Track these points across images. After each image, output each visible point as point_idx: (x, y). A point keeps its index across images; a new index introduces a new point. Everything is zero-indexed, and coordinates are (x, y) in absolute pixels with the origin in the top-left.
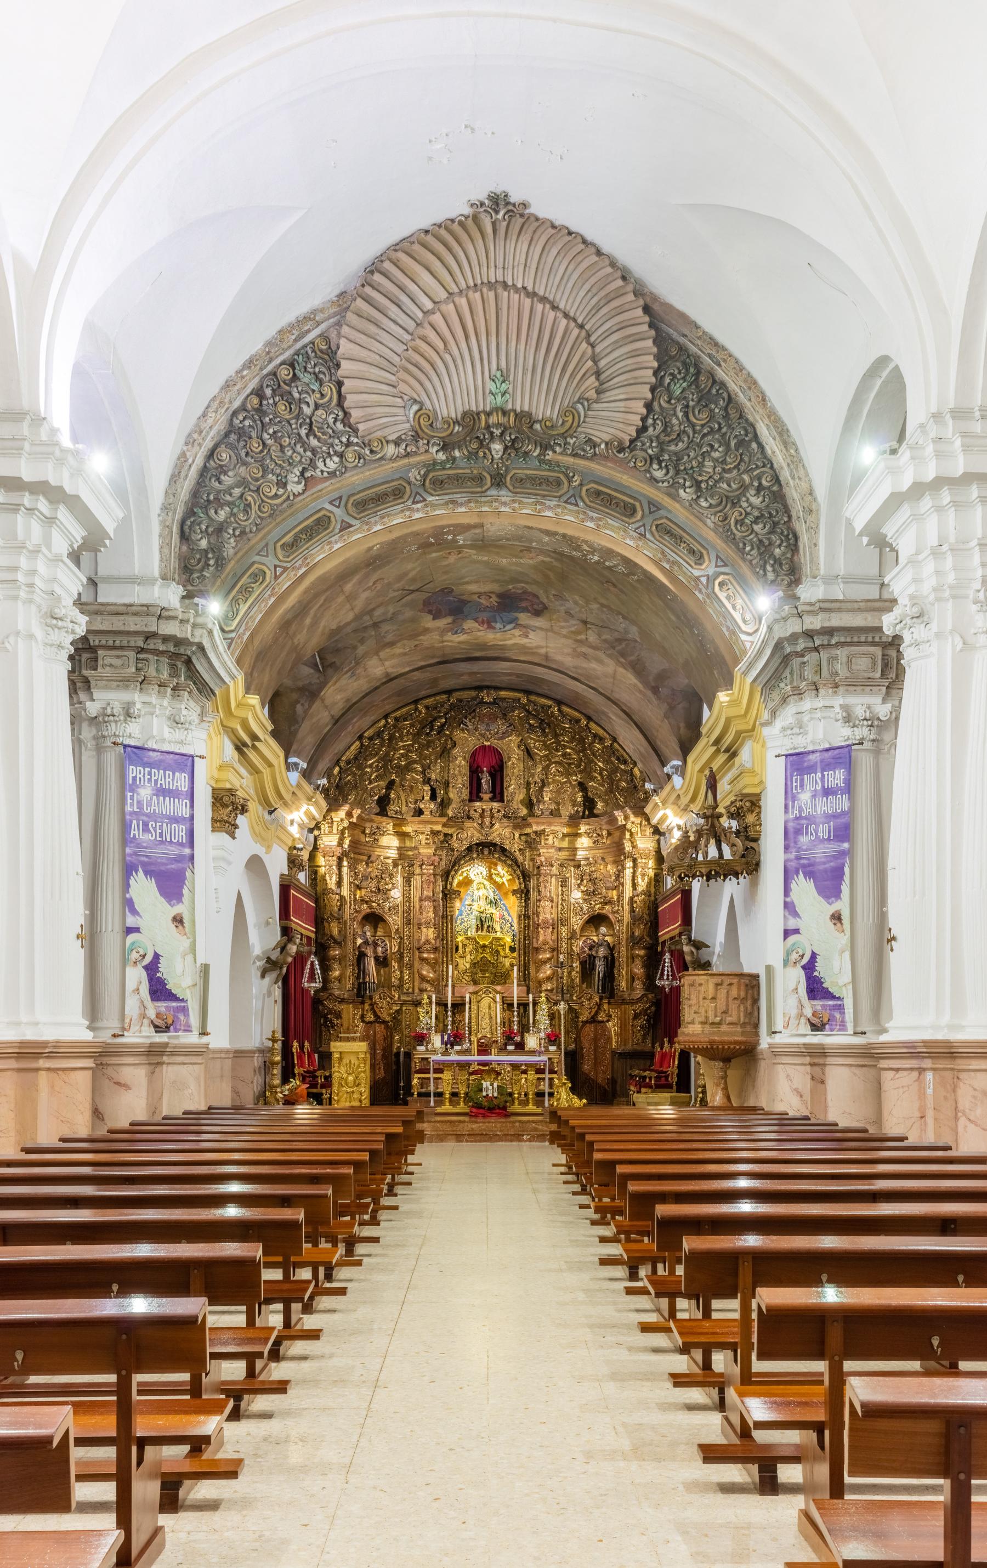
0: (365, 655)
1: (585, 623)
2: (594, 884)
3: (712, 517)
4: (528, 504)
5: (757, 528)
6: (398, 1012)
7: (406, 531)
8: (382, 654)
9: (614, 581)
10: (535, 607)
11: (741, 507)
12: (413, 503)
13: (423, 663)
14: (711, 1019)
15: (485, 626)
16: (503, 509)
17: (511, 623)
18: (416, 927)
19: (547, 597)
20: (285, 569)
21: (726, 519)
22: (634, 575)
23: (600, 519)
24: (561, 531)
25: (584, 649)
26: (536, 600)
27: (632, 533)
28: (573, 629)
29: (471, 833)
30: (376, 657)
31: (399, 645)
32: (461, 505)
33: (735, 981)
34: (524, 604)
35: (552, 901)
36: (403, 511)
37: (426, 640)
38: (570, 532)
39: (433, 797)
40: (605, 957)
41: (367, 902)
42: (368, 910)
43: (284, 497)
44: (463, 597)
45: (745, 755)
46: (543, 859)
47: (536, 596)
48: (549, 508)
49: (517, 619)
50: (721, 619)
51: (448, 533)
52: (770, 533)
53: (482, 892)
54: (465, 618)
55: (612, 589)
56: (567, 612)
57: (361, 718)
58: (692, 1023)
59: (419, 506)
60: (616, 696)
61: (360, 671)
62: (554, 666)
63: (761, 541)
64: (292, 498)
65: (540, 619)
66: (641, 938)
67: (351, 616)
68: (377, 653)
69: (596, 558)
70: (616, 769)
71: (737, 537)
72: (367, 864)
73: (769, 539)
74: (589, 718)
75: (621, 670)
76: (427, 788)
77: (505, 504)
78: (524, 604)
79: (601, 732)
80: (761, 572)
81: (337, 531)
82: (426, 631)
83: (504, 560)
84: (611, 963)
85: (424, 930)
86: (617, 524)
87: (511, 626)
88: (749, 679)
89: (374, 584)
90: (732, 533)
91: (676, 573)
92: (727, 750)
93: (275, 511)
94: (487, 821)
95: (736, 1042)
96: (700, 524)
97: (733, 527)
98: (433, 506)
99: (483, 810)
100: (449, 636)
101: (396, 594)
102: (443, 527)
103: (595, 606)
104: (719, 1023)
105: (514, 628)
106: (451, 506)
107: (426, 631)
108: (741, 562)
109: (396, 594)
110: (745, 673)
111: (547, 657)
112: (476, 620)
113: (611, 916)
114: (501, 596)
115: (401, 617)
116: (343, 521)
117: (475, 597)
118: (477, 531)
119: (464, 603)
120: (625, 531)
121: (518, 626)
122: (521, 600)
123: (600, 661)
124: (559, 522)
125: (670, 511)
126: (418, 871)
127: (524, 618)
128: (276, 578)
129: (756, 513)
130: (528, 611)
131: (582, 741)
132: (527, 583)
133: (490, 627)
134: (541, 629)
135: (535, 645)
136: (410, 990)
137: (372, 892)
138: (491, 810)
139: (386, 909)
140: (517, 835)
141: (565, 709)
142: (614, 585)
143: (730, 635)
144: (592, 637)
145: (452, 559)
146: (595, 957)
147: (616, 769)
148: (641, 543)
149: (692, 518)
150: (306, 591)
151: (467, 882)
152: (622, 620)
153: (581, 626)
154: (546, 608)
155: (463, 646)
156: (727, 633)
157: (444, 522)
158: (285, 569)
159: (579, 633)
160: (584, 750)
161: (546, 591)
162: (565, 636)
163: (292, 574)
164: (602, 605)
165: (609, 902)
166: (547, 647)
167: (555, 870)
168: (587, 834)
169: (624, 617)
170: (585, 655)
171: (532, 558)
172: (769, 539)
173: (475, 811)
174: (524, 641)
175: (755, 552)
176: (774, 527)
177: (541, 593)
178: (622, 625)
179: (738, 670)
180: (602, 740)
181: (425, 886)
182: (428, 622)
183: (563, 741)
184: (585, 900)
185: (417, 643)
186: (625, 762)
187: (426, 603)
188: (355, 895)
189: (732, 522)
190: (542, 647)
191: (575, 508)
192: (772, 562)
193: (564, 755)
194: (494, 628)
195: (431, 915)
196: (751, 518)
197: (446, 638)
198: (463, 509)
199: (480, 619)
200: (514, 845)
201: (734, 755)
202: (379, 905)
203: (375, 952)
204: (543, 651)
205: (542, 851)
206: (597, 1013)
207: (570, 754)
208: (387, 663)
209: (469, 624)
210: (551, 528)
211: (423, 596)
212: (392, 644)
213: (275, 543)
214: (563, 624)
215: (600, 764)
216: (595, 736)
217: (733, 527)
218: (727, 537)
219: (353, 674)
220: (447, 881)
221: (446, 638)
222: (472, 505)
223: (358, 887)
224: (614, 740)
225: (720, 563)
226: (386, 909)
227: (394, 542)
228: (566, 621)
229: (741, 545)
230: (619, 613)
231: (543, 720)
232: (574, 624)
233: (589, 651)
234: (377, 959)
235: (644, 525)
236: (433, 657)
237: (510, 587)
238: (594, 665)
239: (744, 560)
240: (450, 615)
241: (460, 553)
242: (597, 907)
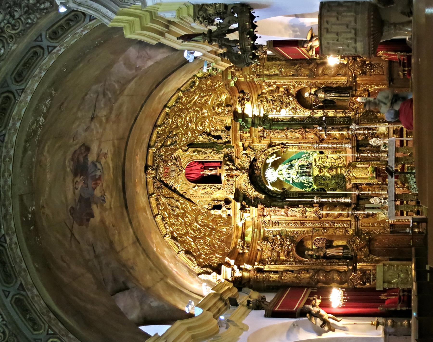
0: (119, 261)
1: (92, 118)
2: (276, 101)
3: (11, 45)
4: (5, 166)
5: (17, 15)
7: (25, 247)
8: (118, 249)
9: (59, 104)
10: (83, 151)
11: (4, 27)
12: (6, 242)
13: (127, 219)
14: (352, 35)
15: (98, 182)
16: (10, 183)
17: (96, 166)
18: (306, 219)
19: (76, 144)
20: (50, 327)
21: (11, 37)
22: (52, 93)
23: (14, 119)
24: (23, 144)
25: (113, 116)
26: (78, 152)
27: (22, 97)
28: (98, 126)
30: (120, 254)
31: (112, 238)
32: (7, 210)
33: (325, 19)
34: (81, 159)
36: (12, 249)
37: (109, 220)
38: (24, 138)
39: (218, 207)
41: (289, 253)
43: (4, 327)
44: (77, 199)
45: (170, 16)
47: (75, 152)
48: (8, 152)
49: (93, 163)
50: (77, 36)
51: (27, 217)
52: (20, 7)
53: (285, 172)
54: (93, 195)
55: (65, 104)
56: (86, 130)
57: (165, 257)
58: (356, 49)
59: (8, 239)
60: (146, 93)
61: (130, 263)
62: (128, 134)
63: (25, 13)
64: (5, 322)
65: (92, 148)
66: (310, 70)
67: (89, 275)
68: (117, 253)
69: (41, 119)
70: (199, 88)
71: (23, 29)
73: (24, 7)
74: (165, 106)
75: (126, 92)
76: (213, 212)
77: (6, 182)
78: (81, 159)
79: (174, 99)
80: (45, 11)
81: (24, 293)
82: (102, 221)
83: (48, 176)
84: (328, 89)
85: (307, 214)
86: (17, 107)
87: (98, 165)
88: (115, 17)
89: (64, 261)
90: (20, 32)
91: (48, 67)
92: (167, 27)
93: (13, 334)
94: (235, 172)
95: (369, 18)
96: (15, 53)
97: (17, 31)
98: (8, 229)
99: (227, 175)
100: (107, 205)
101: (74, 246)
102: (22, 222)
103: (80, 114)
104: (355, 30)
105: (100, 163)
106: (8, 217)
107: (102, 221)
108: (39, 25)
109: (74, 246)
110: (110, 19)
111: (120, 139)
112: (94, 189)
114: (75, 175)
115: (91, 239)
116: (18, 289)
117: (77, 192)
118: (25, 198)
119: (81, 198)
120: (21, 102)
121: (98, 160)
122: (78, 161)
123: (121, 106)
124: (17, 144)
125: (7, 74)
127: (92, 157)
128: (55, 334)
129: (8, 17)
130: (87, 155)
131: (181, 110)
132: (65, 160)
133: (100, 178)
134: (99, 145)
135: (112, 148)
137: (281, 249)
141: (159, 123)
142: (63, 104)
143: (87, 29)
144: (103, 113)
145: (47, 211)
147: (199, 88)
148: (29, 91)
149: (11, 59)
150: (66, 312)
151: (278, 183)
152: (88, 96)
153: (95, 120)
154: (83, 145)
155: (114, 195)
156: (86, 32)
157: (19, 221)
158: (50, 327)
159: (101, 122)
160: (187, 109)
161: (71, 146)
162: (105, 129)
163: (53, 322)
164: (79, 109)
165: (287, 90)
166: (113, 140)
168: (242, 105)
169: (86, 95)
170: (118, 116)
171: (46, 159)
172: (24, 7)
174: (110, 155)
175: (32, 16)
176: (17, 4)
177: (72, 150)
178: (92, 96)
179: (110, 25)
180: (179, 98)
181: (278, 213)
182: (96, 220)
183: (181, 122)
184: (286, 106)
185: (111, 225)
186: (194, 83)
187: (81, 224)
188: (284, 260)
189: (13, 32)
190: (113, 143)
191: (7, 136)
192: (38, 5)
193: (191, 121)
194: (100, 176)
196: (11, 20)
197: (108, 207)
198: (10, 209)
199: (94, 186)
201: (170, 22)
204: (116, 142)
207: (190, 118)
208: (126, 245)
209: (98, 192)
210: (21, 150)
211: (76, 226)
212: (111, 243)
213: (33, 334)
214: (95, 132)
215: (196, 98)
216: (176, 102)
217: (17, 31)
218: (23, 35)
219: (132, 268)
220: (276, 197)
221: (108, 207)
222: (7, 203)
224: (179, 90)
225: (39, 39)
227: (32, 253)
228: (92, 130)
229: (28, 26)
230: (83, 99)
231: (168, 136)
232: (95, 125)
233: (114, 113)
235: (17, 90)
236: (122, 213)
237: (68, 170)
238: (124, 109)
239: (37, 23)
240: (90, 206)
241: (43, 207)
242: (291, 99)
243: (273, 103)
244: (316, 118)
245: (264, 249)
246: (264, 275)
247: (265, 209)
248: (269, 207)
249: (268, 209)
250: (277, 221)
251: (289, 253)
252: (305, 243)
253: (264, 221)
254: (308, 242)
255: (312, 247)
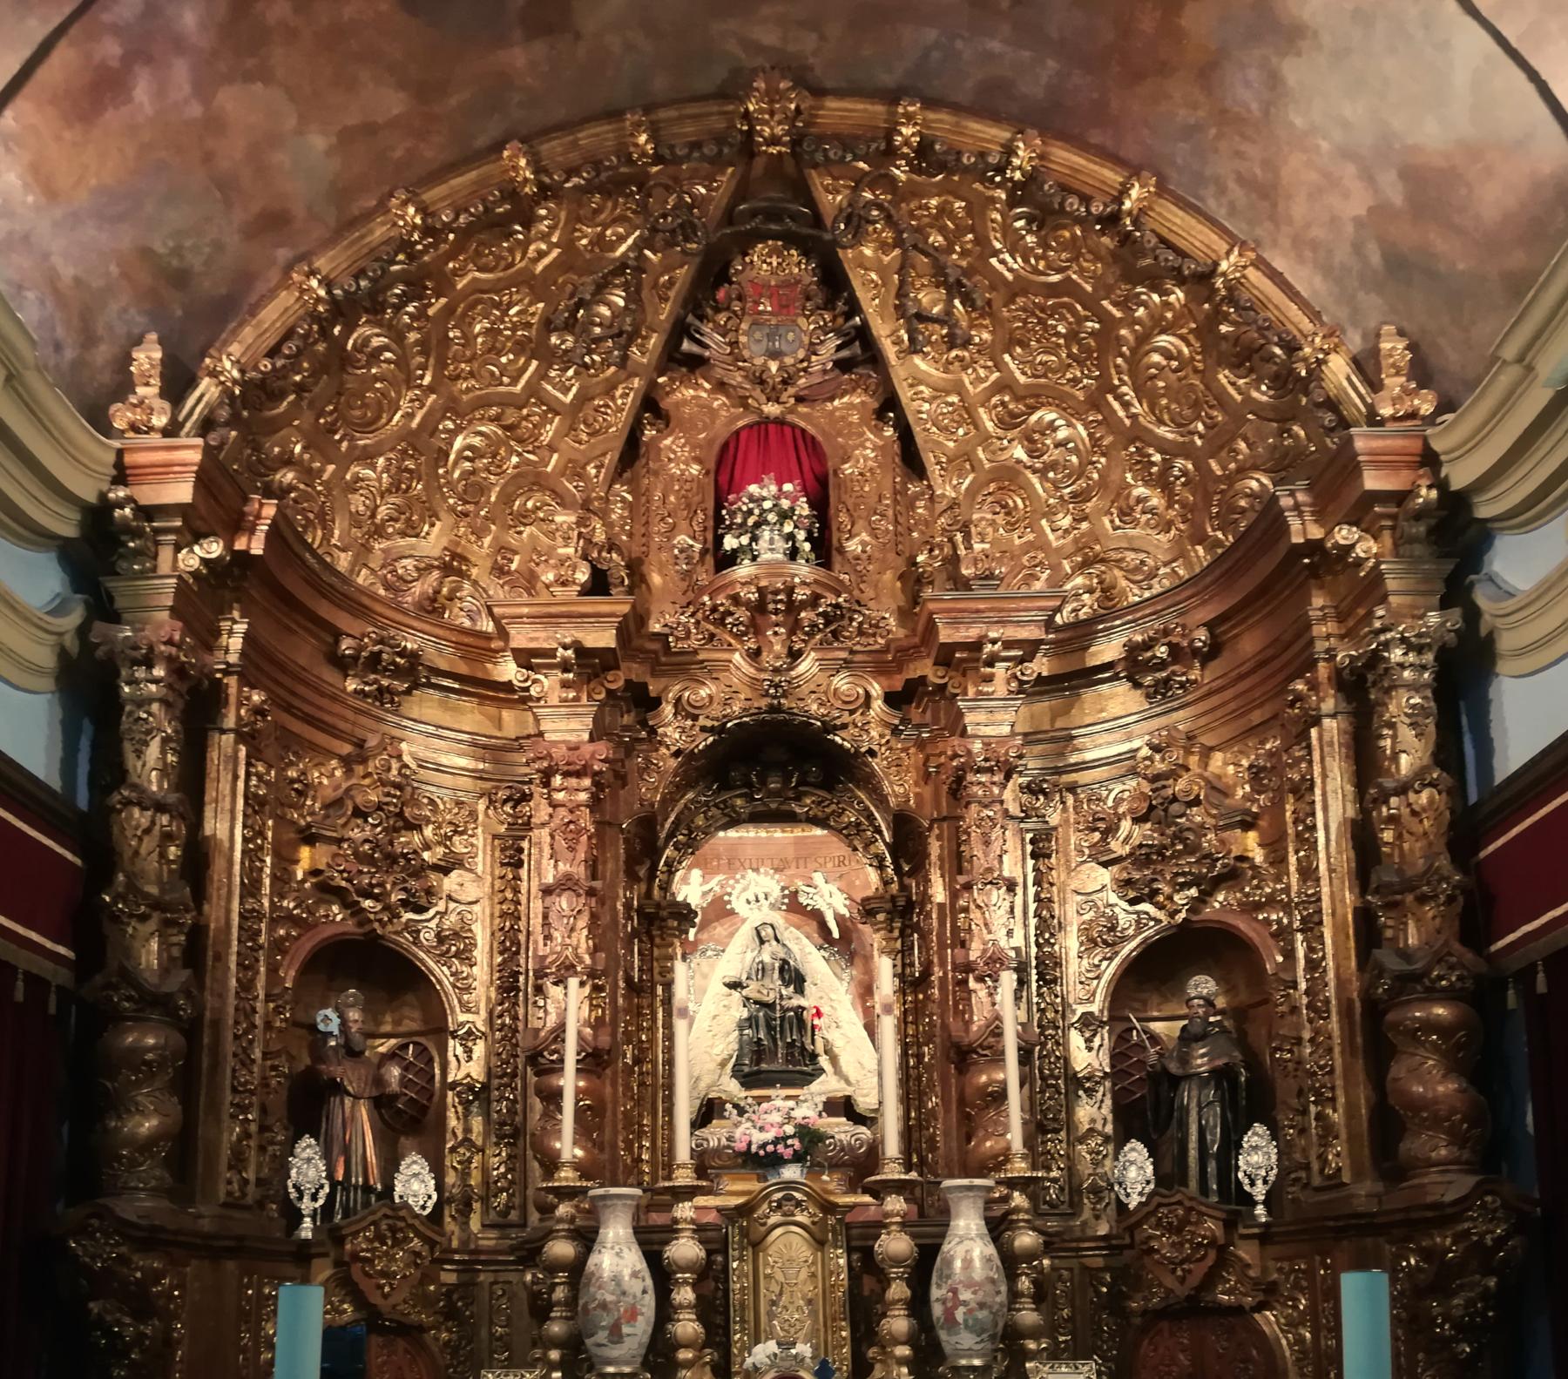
6: (467, 1287)
29: (728, 687)
35: (1011, 887)
40: (1222, 1076)
41: (339, 894)
42: (350, 926)
46: (977, 746)
72: (347, 762)
113: (1242, 925)
126: (541, 812)
136: (514, 1216)
138: (790, 590)
139: (427, 936)
140: (876, 690)
146: (1175, 1082)
167: (1011, 797)
173: (736, 599)
181: (561, 843)
188: (285, 861)
195: (582, 939)
200: (870, 729)
202: (387, 908)
203: (379, 1081)
205: (969, 718)
206: (1211, 1279)
223: (310, 839)
226: (427, 936)
234: (382, 1103)
243: (1151, 808)
244: (1063, 1044)
245: (360, 770)
246: (155, 707)
247: (587, 782)
248: (595, 804)
249: (583, 797)
250: (524, 857)
251: (339, 894)
252: (410, 998)
253: (526, 798)
254: (416, 1014)
255: (388, 1036)
